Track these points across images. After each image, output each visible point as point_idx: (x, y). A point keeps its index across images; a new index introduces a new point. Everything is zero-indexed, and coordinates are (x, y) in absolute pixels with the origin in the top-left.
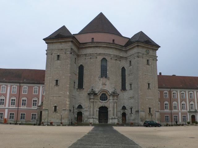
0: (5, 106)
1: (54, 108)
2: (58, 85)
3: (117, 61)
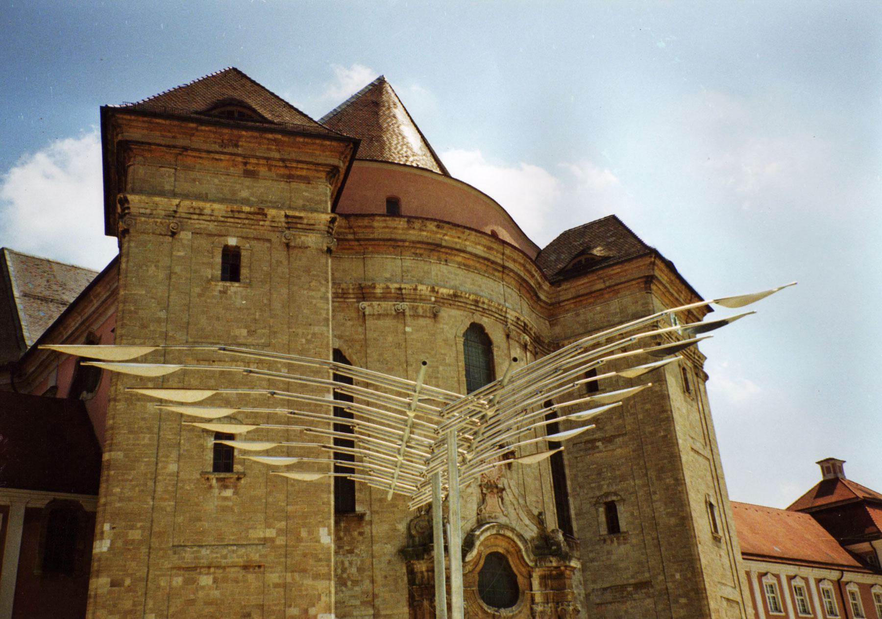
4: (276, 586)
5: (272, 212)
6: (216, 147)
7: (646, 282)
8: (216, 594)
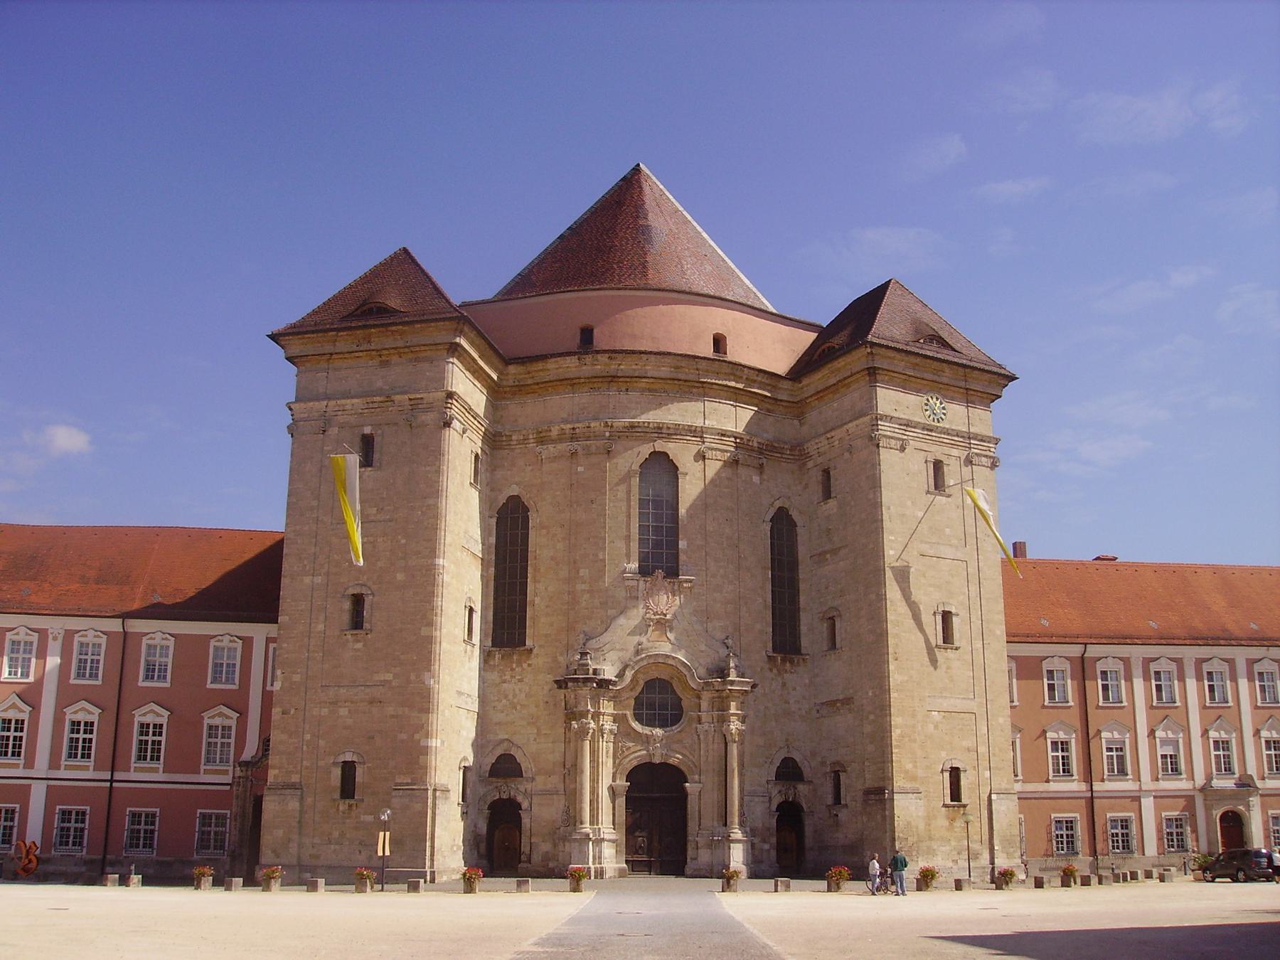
0: (29, 764)
1: (337, 772)
2: (366, 625)
3: (741, 470)
4: (393, 716)
5: (397, 398)
6: (355, 348)
7: (869, 374)
8: (349, 721)
